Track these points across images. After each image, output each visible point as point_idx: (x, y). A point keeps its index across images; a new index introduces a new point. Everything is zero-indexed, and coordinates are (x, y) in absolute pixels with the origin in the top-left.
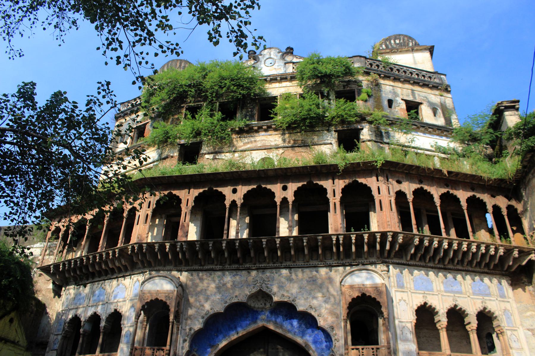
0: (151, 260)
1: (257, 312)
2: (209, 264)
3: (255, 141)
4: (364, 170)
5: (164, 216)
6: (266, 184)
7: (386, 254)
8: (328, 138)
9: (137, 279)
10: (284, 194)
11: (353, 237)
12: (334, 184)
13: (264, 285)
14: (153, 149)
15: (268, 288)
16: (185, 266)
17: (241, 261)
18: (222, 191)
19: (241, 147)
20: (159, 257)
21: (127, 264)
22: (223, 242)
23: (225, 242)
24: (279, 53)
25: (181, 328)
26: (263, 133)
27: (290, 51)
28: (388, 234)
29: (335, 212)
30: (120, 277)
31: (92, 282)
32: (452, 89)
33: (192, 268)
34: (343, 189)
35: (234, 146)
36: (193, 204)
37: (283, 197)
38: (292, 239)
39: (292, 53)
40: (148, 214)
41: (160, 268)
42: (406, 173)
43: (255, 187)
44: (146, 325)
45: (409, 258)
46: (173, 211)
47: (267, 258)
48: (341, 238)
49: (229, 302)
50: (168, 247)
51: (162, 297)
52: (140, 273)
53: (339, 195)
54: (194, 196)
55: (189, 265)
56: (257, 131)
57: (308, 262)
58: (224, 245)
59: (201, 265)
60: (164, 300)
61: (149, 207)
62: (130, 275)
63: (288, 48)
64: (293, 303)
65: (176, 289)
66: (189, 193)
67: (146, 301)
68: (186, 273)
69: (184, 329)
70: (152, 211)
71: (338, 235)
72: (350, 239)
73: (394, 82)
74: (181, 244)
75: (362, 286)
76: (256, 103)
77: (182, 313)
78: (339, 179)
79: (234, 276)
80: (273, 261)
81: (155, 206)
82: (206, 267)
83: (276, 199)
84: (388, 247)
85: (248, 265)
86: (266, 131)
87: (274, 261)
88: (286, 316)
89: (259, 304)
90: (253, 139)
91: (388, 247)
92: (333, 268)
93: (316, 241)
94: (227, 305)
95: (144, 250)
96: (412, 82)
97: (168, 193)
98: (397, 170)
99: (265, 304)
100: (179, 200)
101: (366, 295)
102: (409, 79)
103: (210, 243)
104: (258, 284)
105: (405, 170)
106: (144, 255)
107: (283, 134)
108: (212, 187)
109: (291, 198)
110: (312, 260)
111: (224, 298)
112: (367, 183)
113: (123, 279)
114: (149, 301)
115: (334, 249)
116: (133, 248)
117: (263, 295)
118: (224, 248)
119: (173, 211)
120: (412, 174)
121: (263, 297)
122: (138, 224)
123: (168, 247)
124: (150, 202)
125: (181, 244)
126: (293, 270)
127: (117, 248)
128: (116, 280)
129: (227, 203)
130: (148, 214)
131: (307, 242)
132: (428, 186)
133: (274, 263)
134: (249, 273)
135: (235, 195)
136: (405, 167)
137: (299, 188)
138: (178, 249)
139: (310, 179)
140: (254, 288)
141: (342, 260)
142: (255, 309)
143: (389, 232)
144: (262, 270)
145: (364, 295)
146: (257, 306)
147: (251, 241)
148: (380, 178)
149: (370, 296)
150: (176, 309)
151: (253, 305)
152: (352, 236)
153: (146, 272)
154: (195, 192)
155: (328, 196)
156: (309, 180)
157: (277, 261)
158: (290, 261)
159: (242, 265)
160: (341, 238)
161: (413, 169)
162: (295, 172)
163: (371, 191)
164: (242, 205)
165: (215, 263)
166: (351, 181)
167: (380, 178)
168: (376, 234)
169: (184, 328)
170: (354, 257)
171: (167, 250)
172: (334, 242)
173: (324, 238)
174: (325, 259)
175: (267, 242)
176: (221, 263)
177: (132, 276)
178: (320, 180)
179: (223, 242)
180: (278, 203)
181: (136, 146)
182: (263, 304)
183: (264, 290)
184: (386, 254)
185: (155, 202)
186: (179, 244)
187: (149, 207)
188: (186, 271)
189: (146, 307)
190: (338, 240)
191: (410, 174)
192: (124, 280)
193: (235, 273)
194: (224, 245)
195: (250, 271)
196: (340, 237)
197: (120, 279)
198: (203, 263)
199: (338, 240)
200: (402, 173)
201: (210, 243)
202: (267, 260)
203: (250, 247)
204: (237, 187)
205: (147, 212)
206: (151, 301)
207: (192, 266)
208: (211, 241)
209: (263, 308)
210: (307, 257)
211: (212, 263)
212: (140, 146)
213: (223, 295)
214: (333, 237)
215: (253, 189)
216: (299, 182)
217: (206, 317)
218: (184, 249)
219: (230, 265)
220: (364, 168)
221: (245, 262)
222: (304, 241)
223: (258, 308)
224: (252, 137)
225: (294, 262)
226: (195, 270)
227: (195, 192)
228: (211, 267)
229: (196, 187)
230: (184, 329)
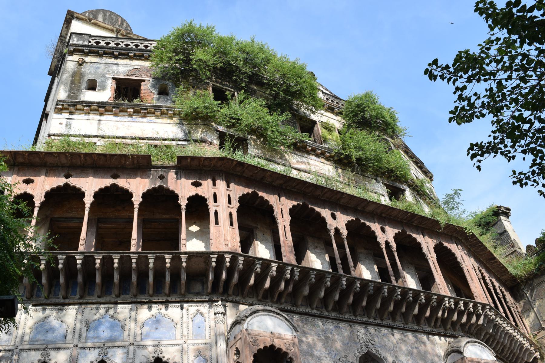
3: (309, 163)
8: (379, 189)
9: (198, 311)
14: (169, 121)
15: (377, 351)
19: (295, 164)
26: (314, 158)
30: (156, 303)
31: (81, 304)
34: (434, 248)
35: (286, 160)
38: (412, 292)
40: (231, 214)
41: (238, 299)
43: (354, 219)
51: (278, 344)
52: (202, 302)
56: (308, 153)
61: (230, 203)
62: (182, 302)
71: (450, 298)
82: (300, 309)
86: (317, 156)
90: (304, 159)
97: (252, 192)
107: (336, 167)
108: (307, 202)
113: (163, 307)
125: (293, 269)
128: (146, 306)
134: (351, 326)
153: (218, 301)
177: (185, 305)
181: (138, 105)
186: (290, 268)
187: (230, 203)
192: (167, 308)
195: (352, 324)
197: (153, 305)
204: (336, 213)
205: (230, 210)
206: (265, 347)
212: (147, 109)
215: (352, 220)
224: (303, 157)
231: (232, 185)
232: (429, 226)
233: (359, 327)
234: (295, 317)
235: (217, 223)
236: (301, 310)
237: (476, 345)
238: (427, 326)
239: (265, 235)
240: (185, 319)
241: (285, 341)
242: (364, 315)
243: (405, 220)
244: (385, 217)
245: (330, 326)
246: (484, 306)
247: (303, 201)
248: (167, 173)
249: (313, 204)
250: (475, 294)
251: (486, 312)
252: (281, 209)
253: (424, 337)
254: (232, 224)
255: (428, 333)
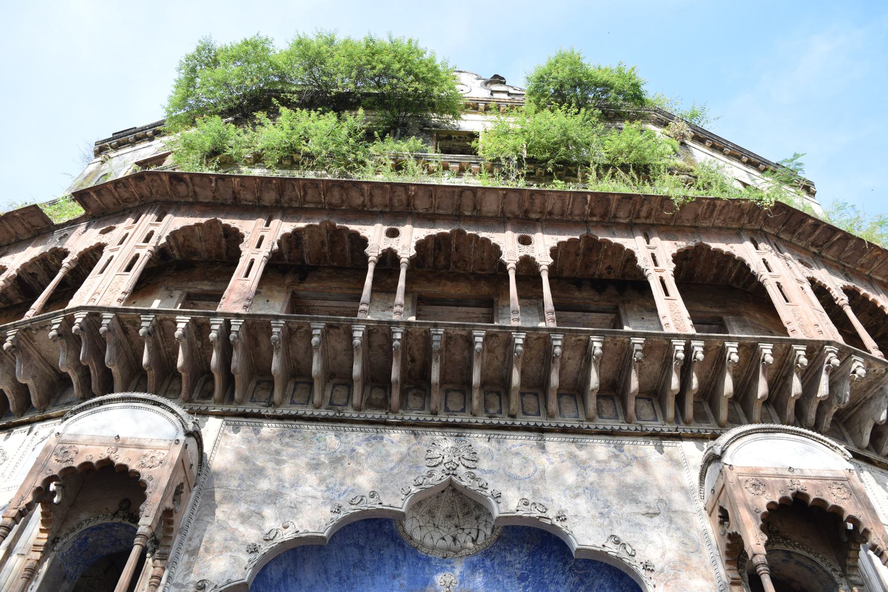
0: (115, 370)
1: (428, 560)
2: (293, 403)
4: (720, 228)
5: (177, 294)
6: (477, 229)
7: (812, 416)
10: (526, 250)
11: (733, 353)
12: (648, 243)
13: (462, 470)
16: (221, 401)
17: (395, 398)
18: (360, 232)
20: (145, 359)
21: (30, 383)
22: (355, 327)
23: (362, 327)
24: (478, 79)
25: (169, 577)
27: (498, 79)
28: (828, 348)
29: (667, 294)
32: (817, 188)
33: (240, 410)
36: (276, 247)
37: (522, 254)
38: (560, 336)
39: (504, 83)
40: (137, 257)
42: (814, 253)
43: (448, 231)
44: (40, 562)
45: (867, 439)
46: (206, 287)
47: (476, 394)
48: (698, 348)
49: (349, 509)
50: (181, 326)
53: (668, 268)
54: (281, 233)
55: (231, 399)
57: (590, 420)
58: (358, 335)
59: (271, 404)
60: (133, 466)
61: (147, 240)
63: (496, 76)
64: (558, 524)
65: (182, 437)
66: (267, 225)
67: (64, 466)
68: (220, 421)
69: (177, 585)
70: (152, 249)
71: (689, 338)
72: (723, 351)
73: (713, 151)
74: (228, 324)
75: (787, 473)
76: (432, 136)
77: (181, 531)
78: (662, 239)
79: (368, 440)
80: (486, 411)
81: (163, 240)
83: (505, 258)
84: (823, 389)
85: (412, 416)
87: (491, 411)
88: (522, 578)
89: (437, 536)
91: (823, 389)
92: (665, 443)
93: (627, 350)
94: (340, 516)
95: (103, 329)
96: (745, 159)
98: (794, 240)
99: (455, 539)
100: (236, 237)
101: (807, 496)
102: (739, 154)
103: (314, 325)
104: (442, 467)
105: (812, 245)
106: (98, 350)
109: (544, 260)
110: (601, 417)
111: (336, 495)
112: (732, 251)
114: (76, 464)
115: (675, 382)
116: (70, 321)
117: (458, 502)
118: (357, 341)
119: (206, 287)
120: (827, 258)
121: (449, 517)
122: (102, 272)
123: (181, 326)
124: (152, 233)
126: (547, 437)
127: (14, 326)
129: (373, 251)
130: (137, 257)
131: (602, 348)
132: (867, 289)
133: (490, 417)
135: (395, 239)
136: (817, 233)
137: (560, 244)
138: (213, 335)
139: (589, 230)
140: (430, 476)
141: (687, 423)
142: (423, 551)
143: (829, 343)
144: (455, 432)
145: (800, 498)
146: (428, 541)
147: (441, 331)
148: (761, 245)
149: (820, 503)
150: (169, 504)
151: (417, 536)
152: (727, 344)
154: (282, 227)
155: (641, 263)
156: (585, 232)
157: (500, 412)
158: (538, 414)
159: (395, 412)
160: (698, 348)
161: (830, 247)
162: (551, 213)
163: (748, 268)
164: (412, 260)
165: (317, 398)
166: (692, 244)
167: (761, 245)
168: (795, 347)
169: (178, 579)
170: (724, 414)
171: (178, 333)
172: (681, 355)
173: (647, 349)
174: (638, 418)
175: (486, 338)
176: (331, 403)
177: (38, 427)
178: (614, 235)
179: (355, 327)
180: (511, 265)
182: (449, 540)
183: (463, 484)
184: (812, 416)
185: (167, 234)
186: (221, 320)
187: (147, 240)
188: (218, 415)
189: (56, 500)
190: (688, 350)
191: (823, 257)
193: (370, 428)
194: (358, 335)
196: (694, 343)
198: (277, 396)
199: (688, 350)
200: (805, 250)
201: (314, 325)
202: (476, 403)
203: (436, 345)
207: (241, 402)
208: (318, 320)
209: (449, 549)
210: (592, 403)
211: (309, 400)
213: (328, 489)
214: (675, 342)
216: (559, 234)
217: (265, 548)
218: (233, 335)
219: (358, 409)
220: (718, 223)
221: (404, 405)
222: (595, 344)
223: (434, 548)
225: (551, 416)
226: (245, 415)
227: (282, 227)
228: (300, 413)
229: (286, 211)
230: (177, 585)
231: (169, 216)
232: (653, 217)
233: (438, 435)
234: (268, 429)
235: (102, 272)
236: (286, 412)
237: (779, 438)
238: (661, 421)
239: (271, 302)
240: (22, 449)
241: (146, 451)
242: (463, 411)
243: (592, 214)
244: (537, 220)
245: (355, 439)
246: (815, 349)
247: (325, 219)
248: (74, 229)
249: (349, 221)
250: (789, 328)
251: (829, 362)
252: (262, 238)
253: (648, 449)
254: (129, 269)
255: (659, 436)
